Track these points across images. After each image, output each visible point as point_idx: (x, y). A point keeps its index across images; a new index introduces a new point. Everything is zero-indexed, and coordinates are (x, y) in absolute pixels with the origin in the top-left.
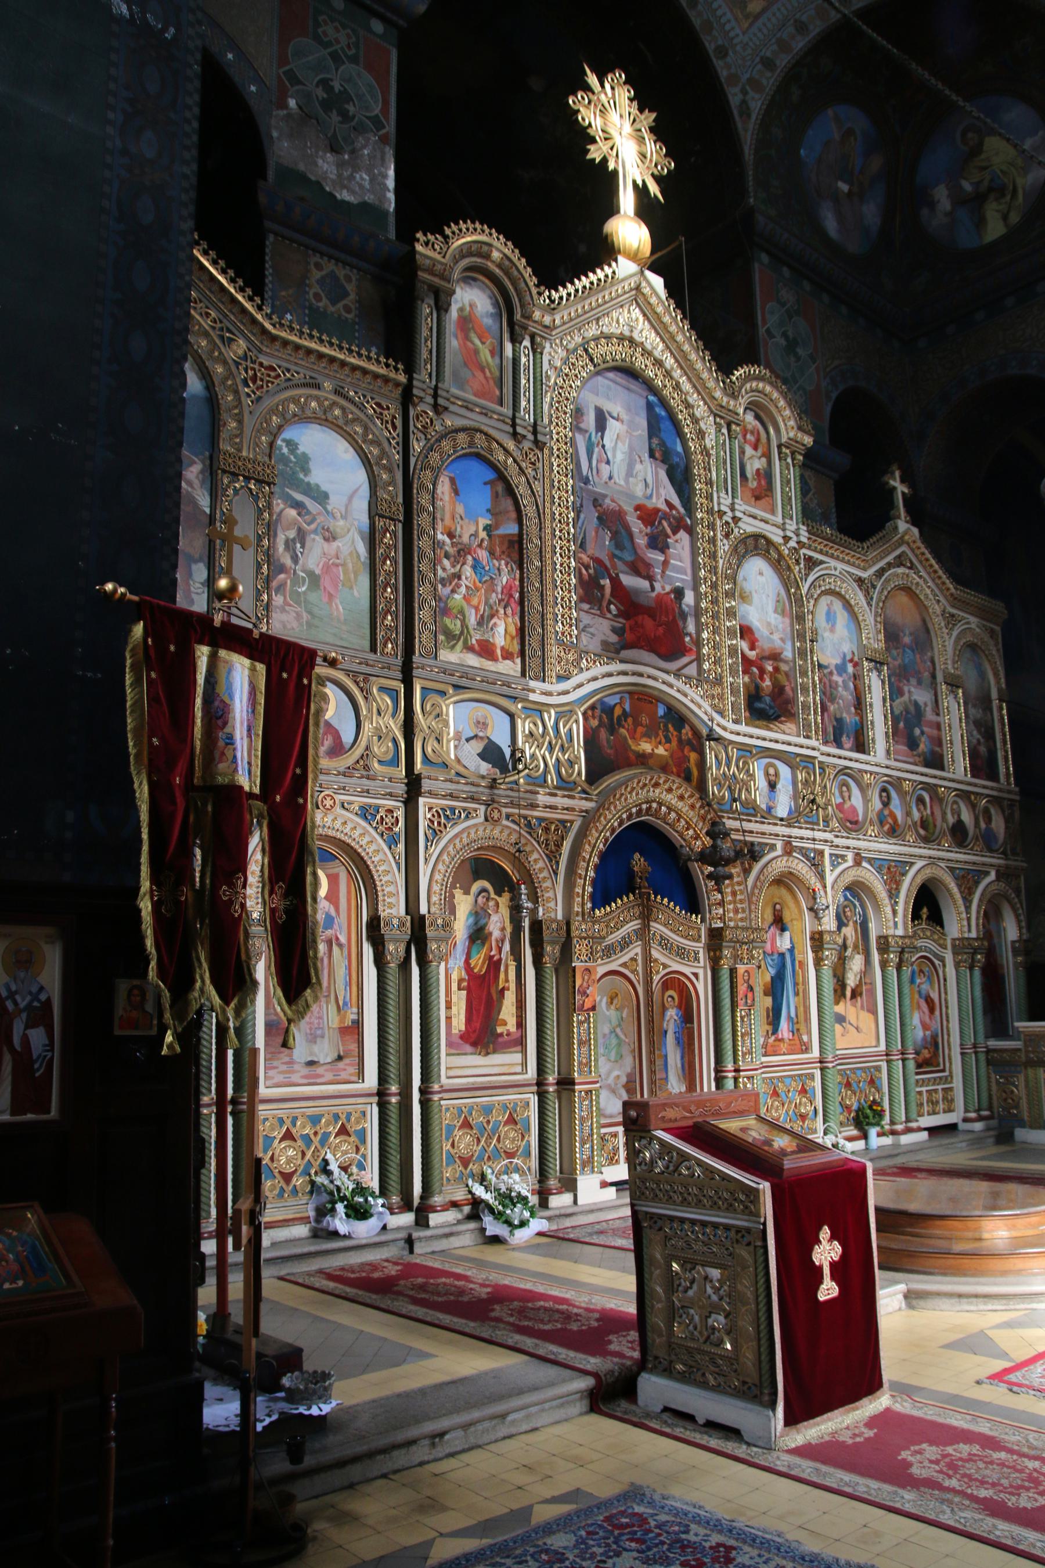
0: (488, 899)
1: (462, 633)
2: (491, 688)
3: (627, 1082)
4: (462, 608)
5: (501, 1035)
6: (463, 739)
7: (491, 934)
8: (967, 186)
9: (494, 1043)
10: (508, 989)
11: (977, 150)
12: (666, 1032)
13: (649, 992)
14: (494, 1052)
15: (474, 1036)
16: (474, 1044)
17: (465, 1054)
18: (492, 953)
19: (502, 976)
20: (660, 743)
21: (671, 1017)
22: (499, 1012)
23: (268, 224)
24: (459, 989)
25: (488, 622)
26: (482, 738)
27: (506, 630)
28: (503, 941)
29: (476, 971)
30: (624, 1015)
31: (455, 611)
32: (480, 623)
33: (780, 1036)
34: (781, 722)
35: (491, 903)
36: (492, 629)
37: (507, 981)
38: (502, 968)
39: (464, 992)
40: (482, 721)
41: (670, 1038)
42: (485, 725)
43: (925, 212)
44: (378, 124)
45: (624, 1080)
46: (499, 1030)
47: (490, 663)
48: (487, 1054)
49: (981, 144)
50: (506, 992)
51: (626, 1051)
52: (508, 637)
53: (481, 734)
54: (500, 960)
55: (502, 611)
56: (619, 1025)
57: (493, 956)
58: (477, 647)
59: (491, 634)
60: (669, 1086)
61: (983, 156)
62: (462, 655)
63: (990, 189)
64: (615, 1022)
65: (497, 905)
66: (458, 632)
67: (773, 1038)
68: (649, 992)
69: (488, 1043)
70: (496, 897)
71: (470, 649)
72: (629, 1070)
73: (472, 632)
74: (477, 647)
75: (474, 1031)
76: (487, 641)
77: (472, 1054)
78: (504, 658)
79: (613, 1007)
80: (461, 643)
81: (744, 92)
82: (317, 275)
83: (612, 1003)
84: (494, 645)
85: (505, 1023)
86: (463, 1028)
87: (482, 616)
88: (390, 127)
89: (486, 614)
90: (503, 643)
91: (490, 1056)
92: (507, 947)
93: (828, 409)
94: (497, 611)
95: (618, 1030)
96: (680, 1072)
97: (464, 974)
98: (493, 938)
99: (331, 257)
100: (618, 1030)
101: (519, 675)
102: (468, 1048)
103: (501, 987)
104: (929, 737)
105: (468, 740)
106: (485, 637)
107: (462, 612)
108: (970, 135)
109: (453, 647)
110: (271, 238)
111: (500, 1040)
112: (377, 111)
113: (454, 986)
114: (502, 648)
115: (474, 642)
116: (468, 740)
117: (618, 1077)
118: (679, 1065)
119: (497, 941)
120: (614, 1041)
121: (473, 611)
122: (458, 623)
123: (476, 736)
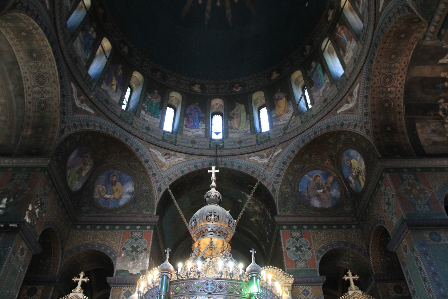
8: (354, 174)
11: (351, 165)
23: (111, 285)
43: (350, 184)
44: (146, 249)
49: (351, 163)
61: (353, 165)
63: (358, 173)
81: (273, 186)
82: (123, 292)
88: (149, 249)
93: (318, 263)
99: (129, 287)
108: (348, 161)
110: (112, 288)
112: (146, 246)
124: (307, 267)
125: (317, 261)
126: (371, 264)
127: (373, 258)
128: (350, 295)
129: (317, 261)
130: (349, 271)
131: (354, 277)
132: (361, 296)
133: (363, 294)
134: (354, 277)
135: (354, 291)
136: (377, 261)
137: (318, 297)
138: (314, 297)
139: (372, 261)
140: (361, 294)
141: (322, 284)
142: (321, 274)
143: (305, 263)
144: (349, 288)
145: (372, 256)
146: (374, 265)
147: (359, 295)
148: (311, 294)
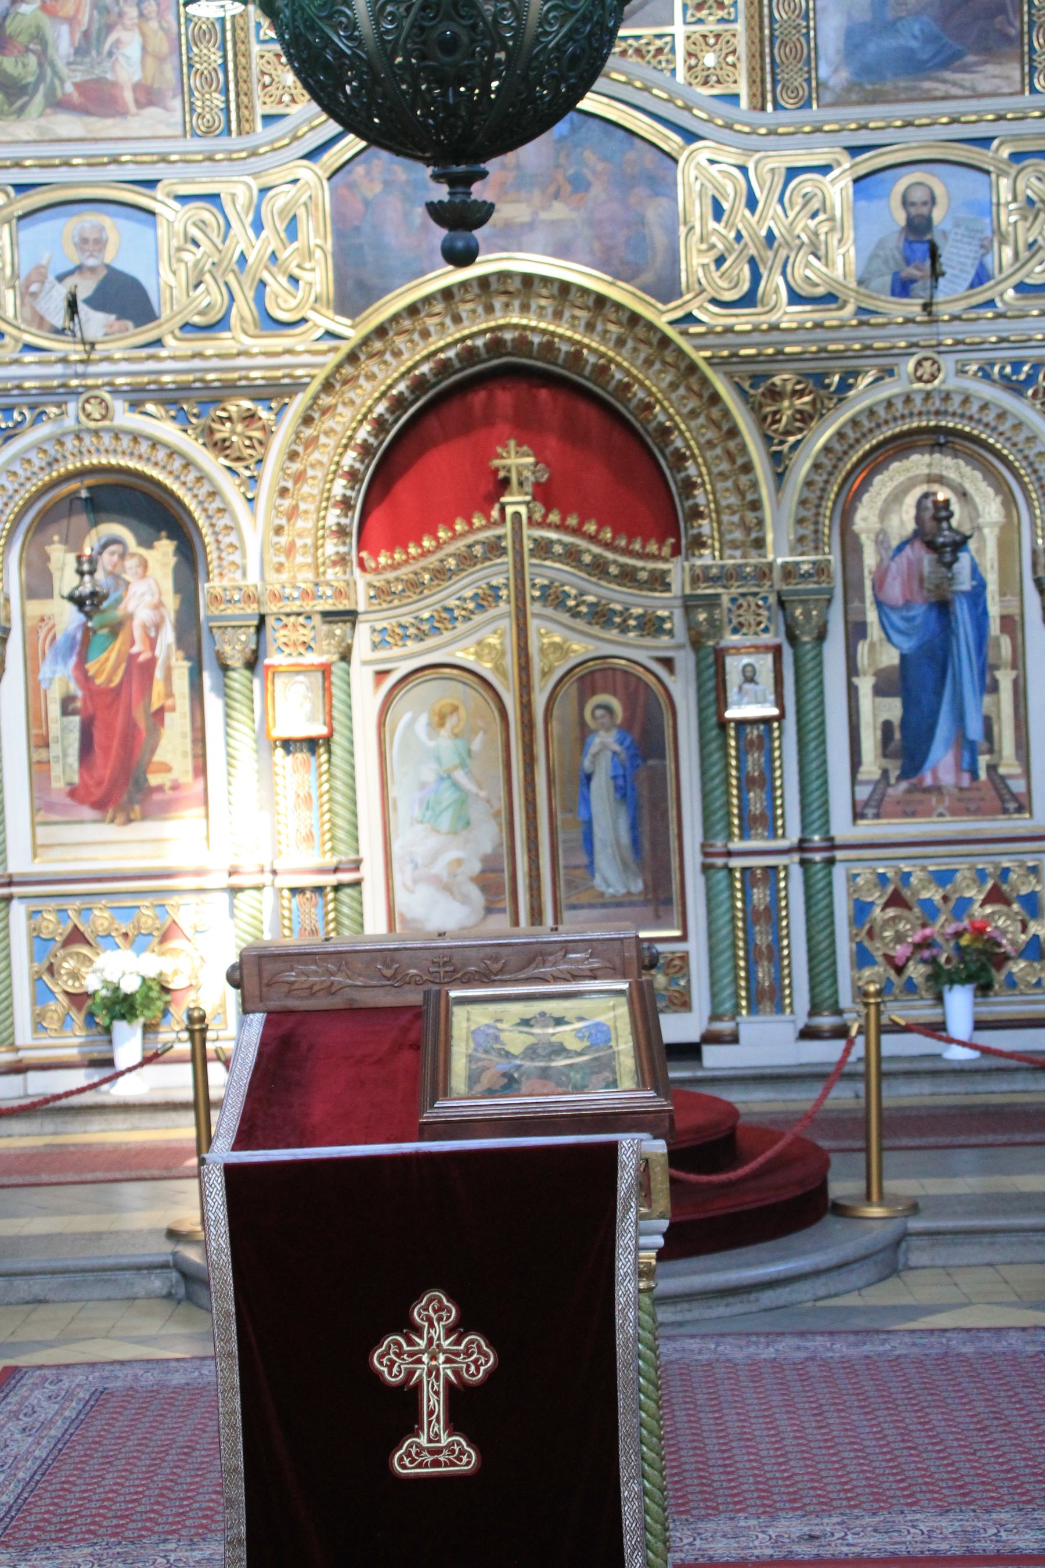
0: (123, 556)
1: (41, 78)
2: (114, 172)
3: (483, 872)
4: (39, 28)
5: (160, 788)
6: (51, 278)
7: (130, 617)
9: (141, 802)
10: (173, 709)
12: (589, 778)
13: (526, 706)
14: (145, 817)
15: (98, 793)
16: (100, 805)
17: (81, 822)
18: (135, 649)
19: (158, 686)
20: (556, 196)
21: (604, 747)
22: (153, 751)
24: (66, 711)
25: (100, 42)
26: (93, 270)
27: (144, 49)
28: (158, 627)
29: (99, 681)
30: (476, 744)
31: (23, 39)
32: (81, 51)
33: (928, 781)
34: (965, 69)
35: (130, 563)
36: (110, 54)
37: (169, 694)
38: (159, 674)
39: (76, 720)
40: (91, 236)
41: (601, 789)
42: (100, 243)
45: (476, 867)
46: (154, 780)
47: (109, 122)
48: (129, 821)
50: (168, 717)
51: (477, 812)
52: (150, 61)
53: (91, 262)
54: (152, 662)
55: (132, 12)
56: (463, 765)
57: (138, 654)
58: (76, 97)
59: (107, 64)
60: (598, 880)
62: (43, 121)
64: (450, 759)
65: (144, 564)
66: (31, 79)
67: (904, 785)
68: (526, 706)
69: (131, 802)
70: (142, 551)
71: (58, 104)
72: (488, 848)
73: (64, 71)
74: (76, 97)
75: (99, 784)
76: (100, 81)
77: (95, 821)
78: (140, 105)
79: (444, 732)
80: (39, 99)
83: (441, 724)
84: (114, 84)
85: (167, 768)
86: (76, 779)
87: (86, 34)
89: (95, 26)
90: (137, 77)
91: (134, 825)
92: (168, 636)
94: (121, 15)
95: (460, 775)
96: (628, 854)
97: (75, 689)
98: (136, 624)
100: (460, 775)
101: (179, 131)
102: (87, 812)
103: (155, 705)
105: (61, 278)
106: (97, 72)
107: (39, 37)
109: (21, 111)
111: (157, 797)
113: (54, 709)
114: (137, 87)
115: (69, 88)
116: (61, 278)
117: (459, 862)
118: (625, 839)
119: (145, 628)
120: (448, 796)
121: (65, 29)
122: (32, 60)
123: (79, 269)
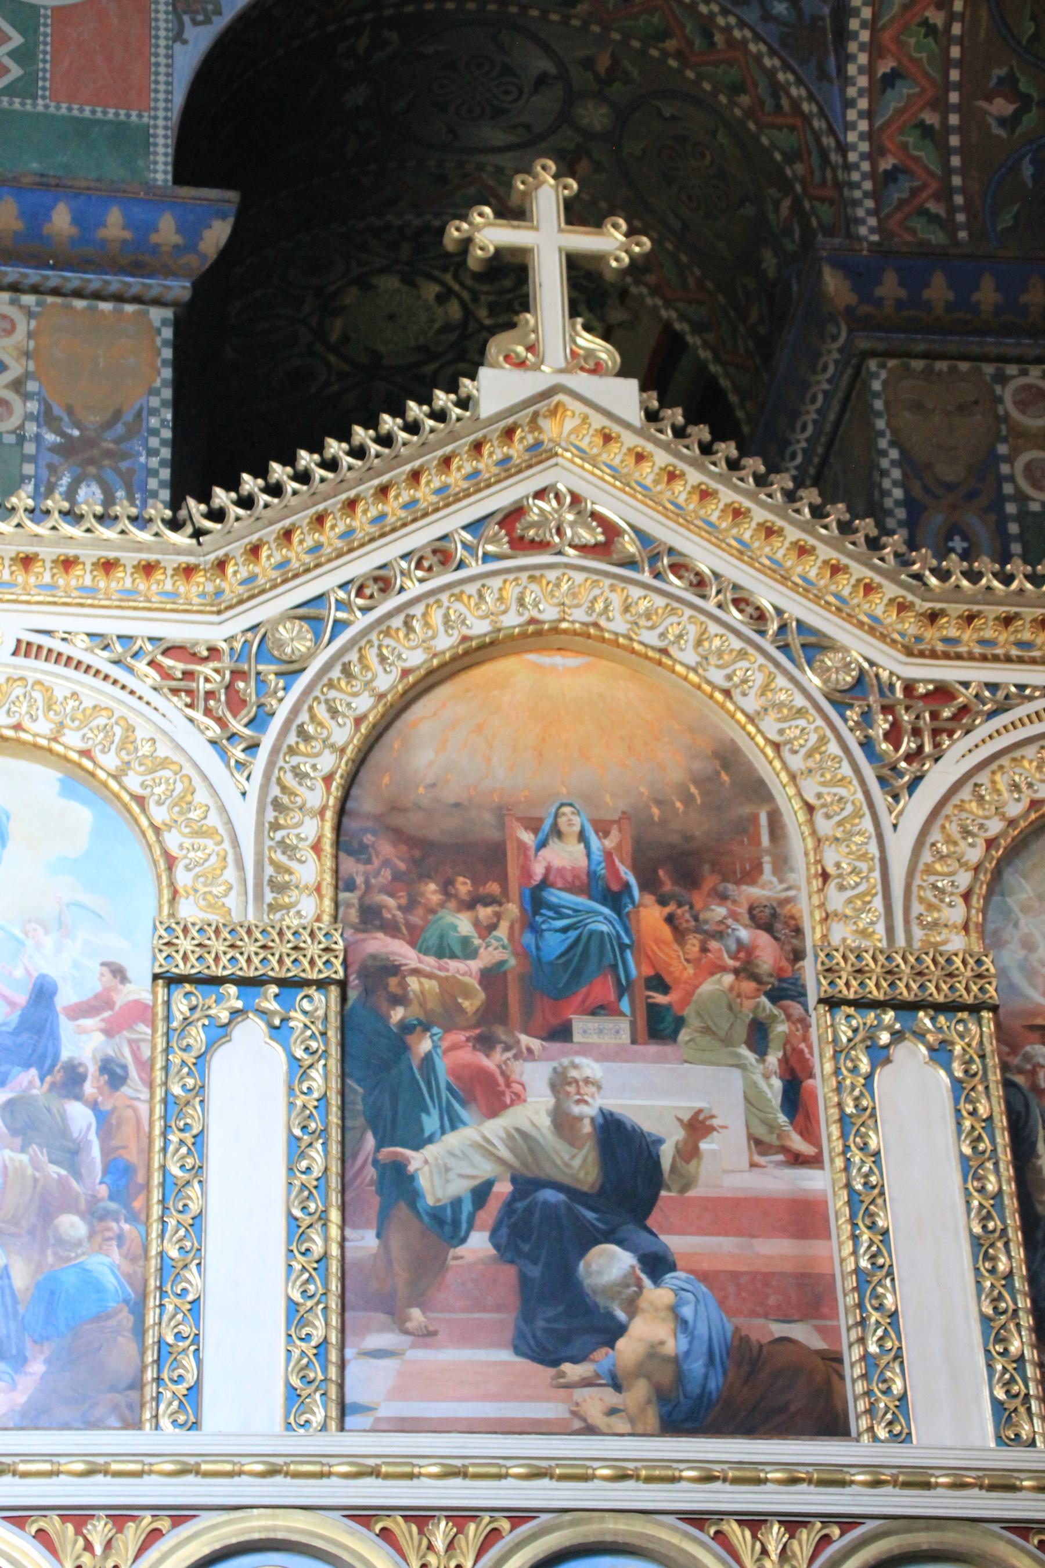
104: (704, 1277)
124: (25, 88)
125: (178, 37)
126: (843, 148)
127: (890, 80)
128: (487, 408)
129: (178, 37)
130: (546, 170)
131: (584, 241)
132: (630, 440)
133: (652, 416)
134: (584, 241)
135: (545, 377)
136: (931, 118)
137: (94, 419)
138: (47, 418)
139: (869, 115)
140: (636, 417)
141: (180, 289)
142: (180, 178)
143: (17, 40)
144: (495, 347)
145: (875, 50)
146: (887, 164)
147: (598, 421)
148: (17, 385)
